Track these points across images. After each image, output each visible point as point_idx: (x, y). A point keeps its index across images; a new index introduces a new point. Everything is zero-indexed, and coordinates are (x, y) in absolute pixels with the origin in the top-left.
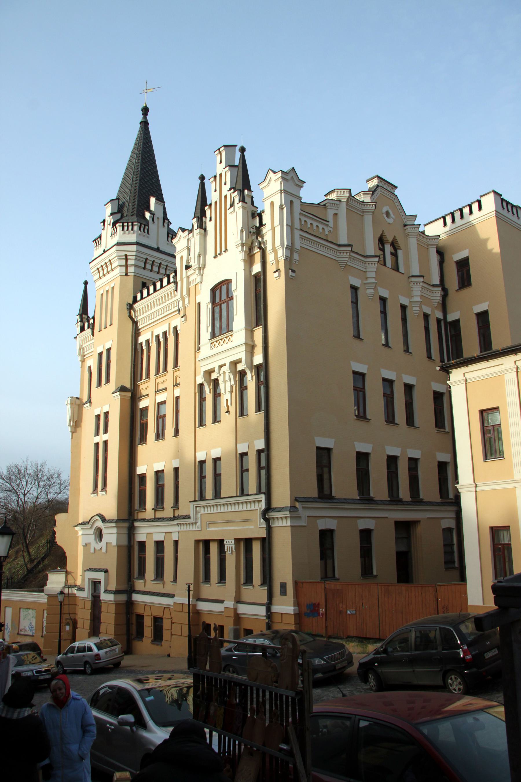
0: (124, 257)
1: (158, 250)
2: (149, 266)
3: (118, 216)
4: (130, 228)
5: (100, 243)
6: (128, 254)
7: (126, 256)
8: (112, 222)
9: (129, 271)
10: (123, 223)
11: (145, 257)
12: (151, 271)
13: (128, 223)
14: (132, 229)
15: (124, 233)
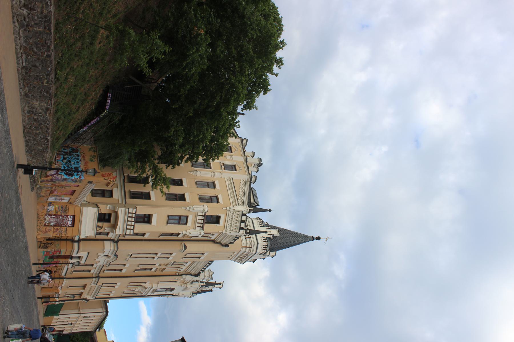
0: (251, 247)
1: (251, 258)
2: (243, 255)
3: (272, 237)
4: (264, 249)
5: (261, 225)
6: (252, 249)
7: (251, 248)
8: (269, 236)
9: (243, 248)
10: (267, 245)
11: (248, 255)
12: (241, 255)
13: (267, 248)
14: (263, 250)
15: (262, 245)
